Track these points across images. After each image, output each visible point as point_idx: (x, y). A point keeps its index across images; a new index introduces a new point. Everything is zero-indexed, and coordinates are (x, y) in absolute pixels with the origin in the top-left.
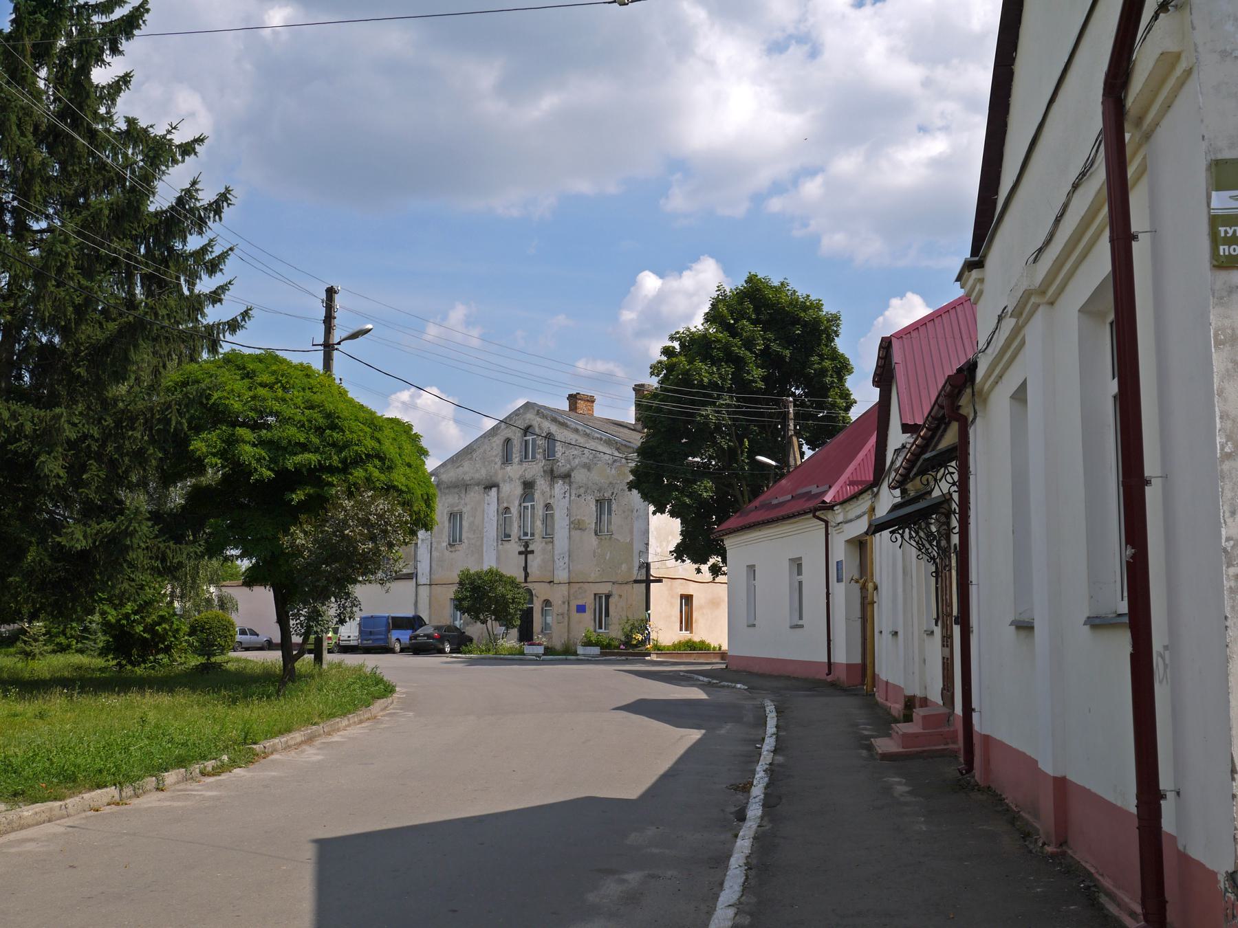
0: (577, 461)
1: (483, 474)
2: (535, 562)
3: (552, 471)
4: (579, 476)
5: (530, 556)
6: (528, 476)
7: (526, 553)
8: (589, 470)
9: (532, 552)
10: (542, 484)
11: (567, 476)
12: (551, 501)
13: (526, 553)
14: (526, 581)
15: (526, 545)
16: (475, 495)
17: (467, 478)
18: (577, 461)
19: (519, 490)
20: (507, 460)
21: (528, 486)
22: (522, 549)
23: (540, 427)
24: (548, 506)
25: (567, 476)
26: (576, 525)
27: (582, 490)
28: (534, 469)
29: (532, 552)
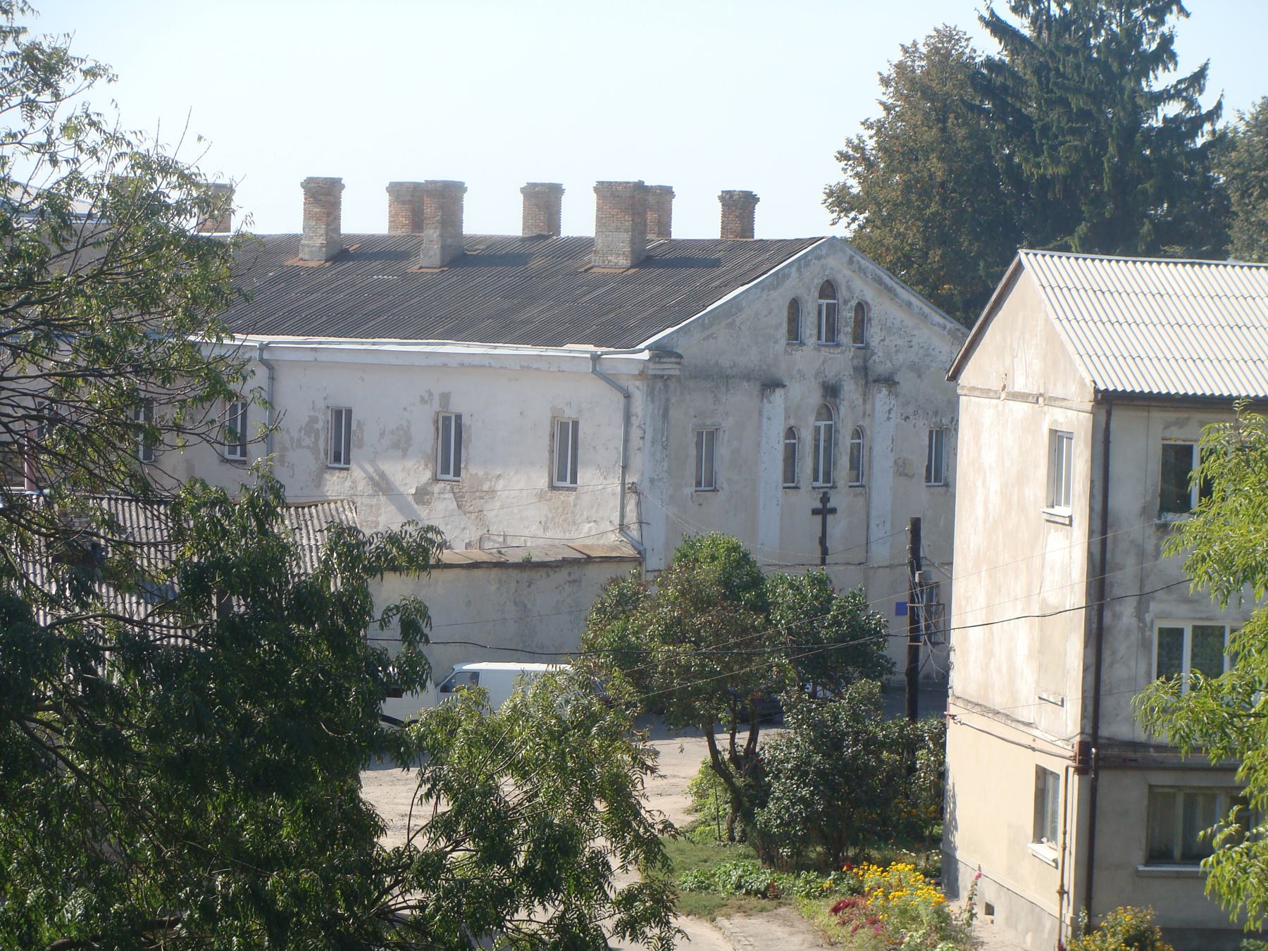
0: (901, 357)
1: (752, 359)
2: (838, 527)
3: (866, 368)
4: (906, 382)
5: (830, 518)
6: (830, 375)
7: (824, 511)
8: (919, 376)
9: (833, 511)
10: (851, 390)
11: (889, 381)
12: (865, 423)
13: (824, 511)
14: (823, 562)
15: (825, 499)
16: (741, 398)
17: (725, 362)
18: (901, 357)
19: (815, 398)
20: (794, 334)
21: (831, 391)
22: (820, 506)
23: (849, 288)
24: (858, 433)
25: (889, 381)
26: (902, 469)
27: (910, 410)
28: (840, 362)
29: (833, 511)
